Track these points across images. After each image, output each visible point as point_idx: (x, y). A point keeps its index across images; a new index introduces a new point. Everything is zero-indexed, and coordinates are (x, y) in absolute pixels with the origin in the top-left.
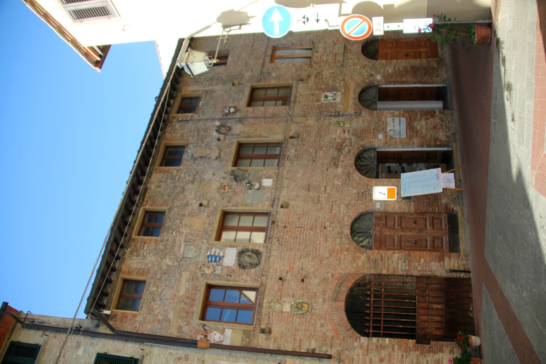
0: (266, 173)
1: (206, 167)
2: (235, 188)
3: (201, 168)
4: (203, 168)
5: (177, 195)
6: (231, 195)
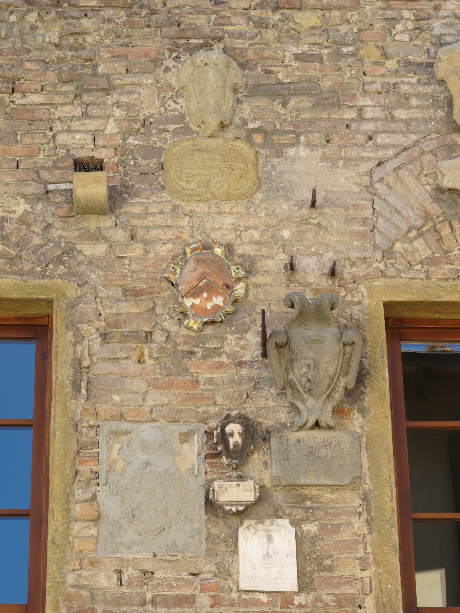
0: (344, 536)
1: (378, 147)
2: (217, 351)
3: (369, 114)
4: (367, 127)
5: (161, 17)
6: (159, 337)
